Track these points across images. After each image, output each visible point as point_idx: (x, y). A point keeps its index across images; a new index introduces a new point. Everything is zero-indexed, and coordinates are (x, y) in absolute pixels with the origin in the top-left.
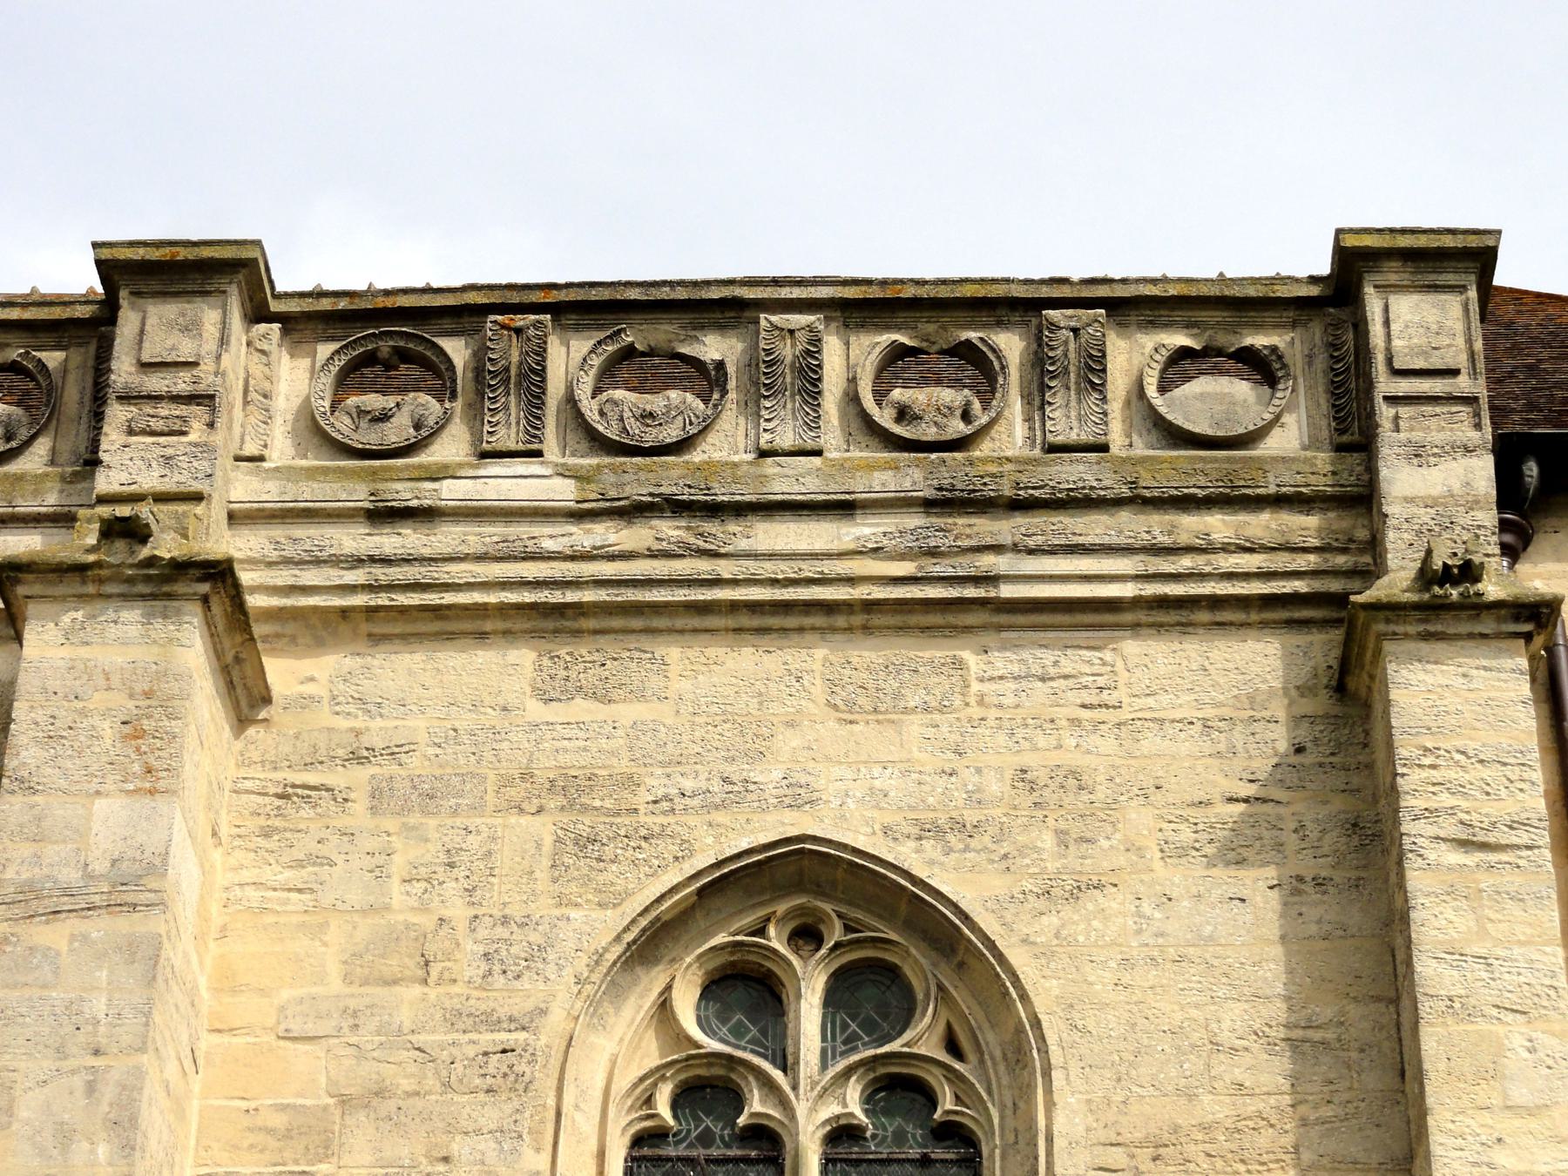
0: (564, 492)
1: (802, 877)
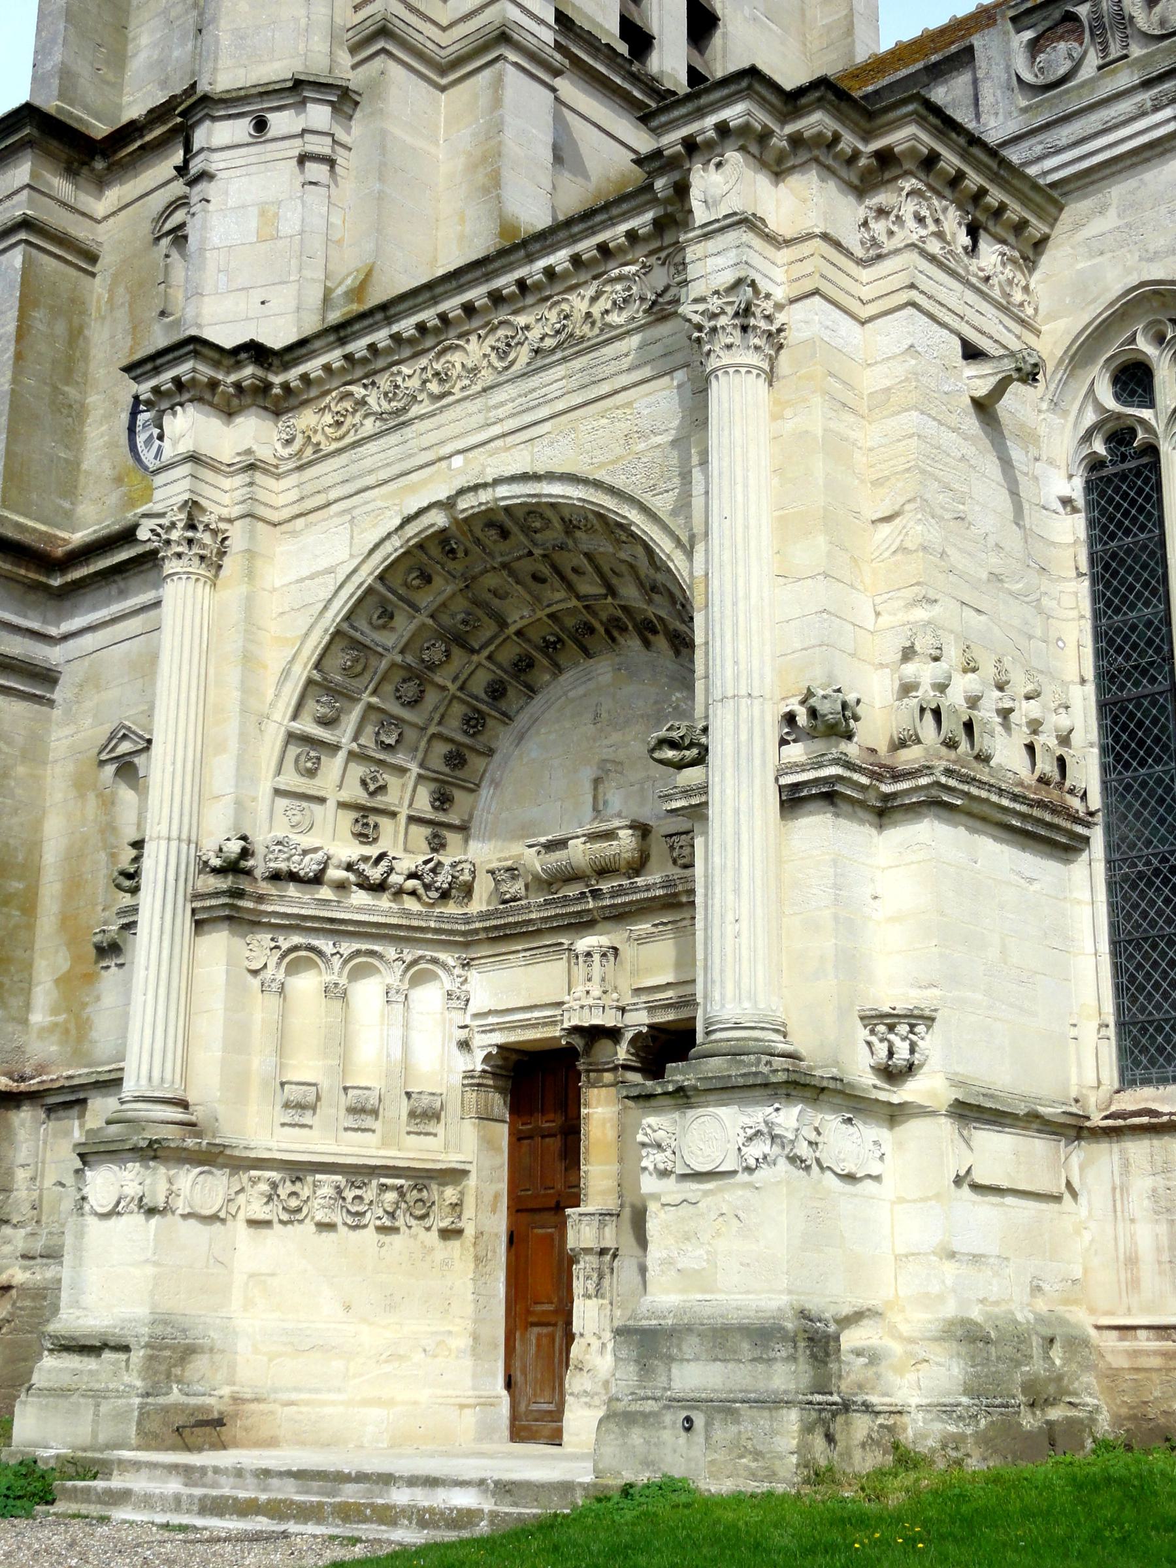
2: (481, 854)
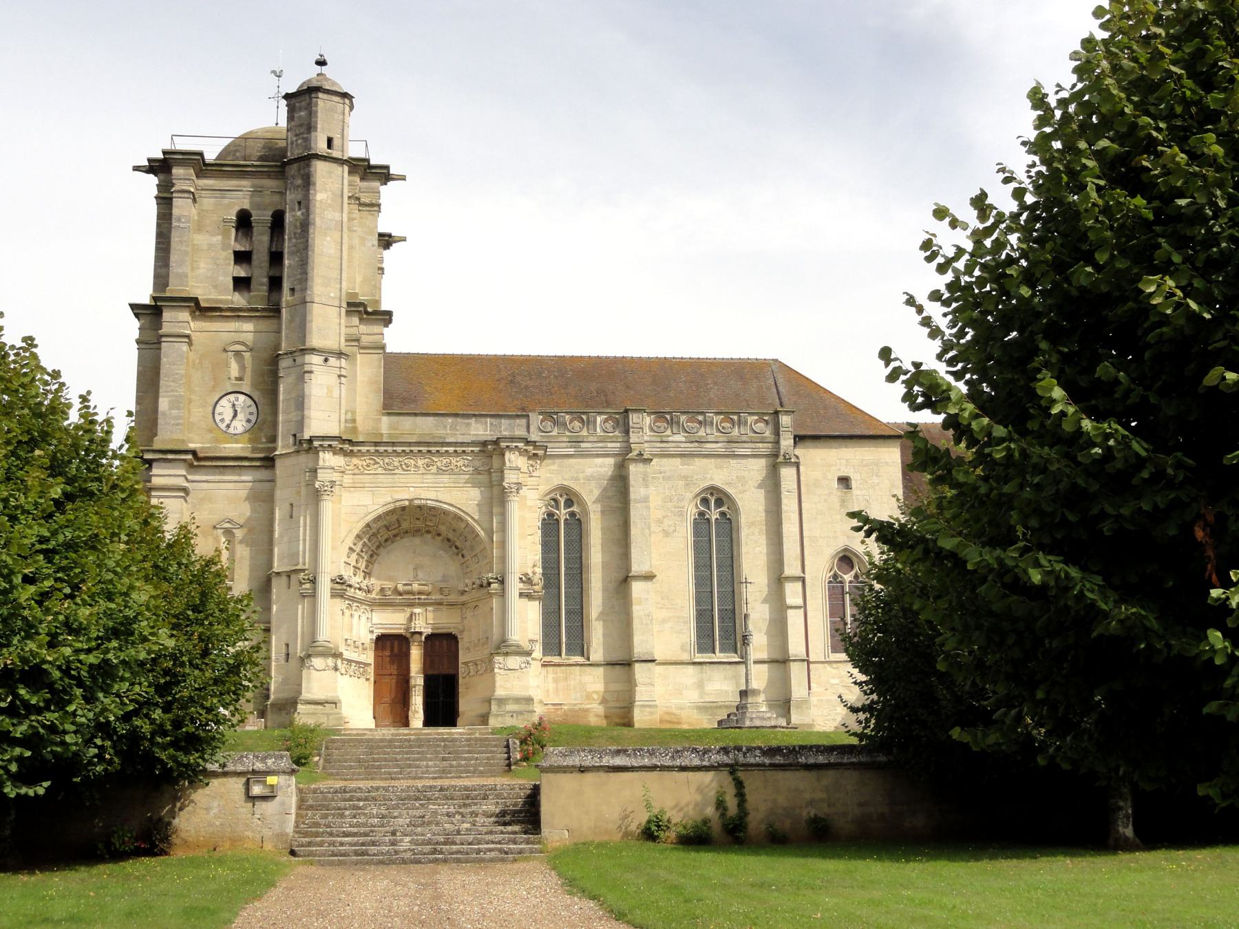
1: (713, 490)
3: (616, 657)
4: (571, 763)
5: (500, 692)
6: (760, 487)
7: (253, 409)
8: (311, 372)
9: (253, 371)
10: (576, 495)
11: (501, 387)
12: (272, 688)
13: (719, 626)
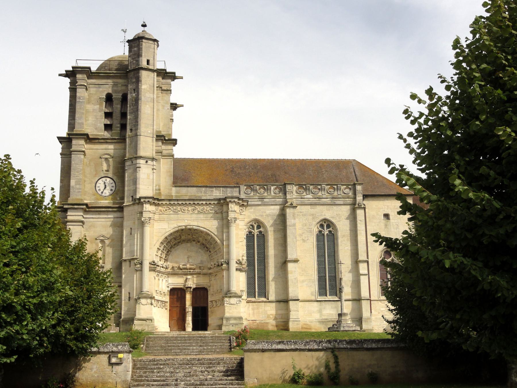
0: (312, 197)
1: (325, 220)
2: (170, 264)
3: (281, 298)
4: (258, 348)
5: (227, 315)
6: (347, 219)
7: (114, 185)
8: (140, 167)
9: (113, 167)
10: (262, 223)
11: (227, 173)
12: (123, 313)
13: (329, 283)
